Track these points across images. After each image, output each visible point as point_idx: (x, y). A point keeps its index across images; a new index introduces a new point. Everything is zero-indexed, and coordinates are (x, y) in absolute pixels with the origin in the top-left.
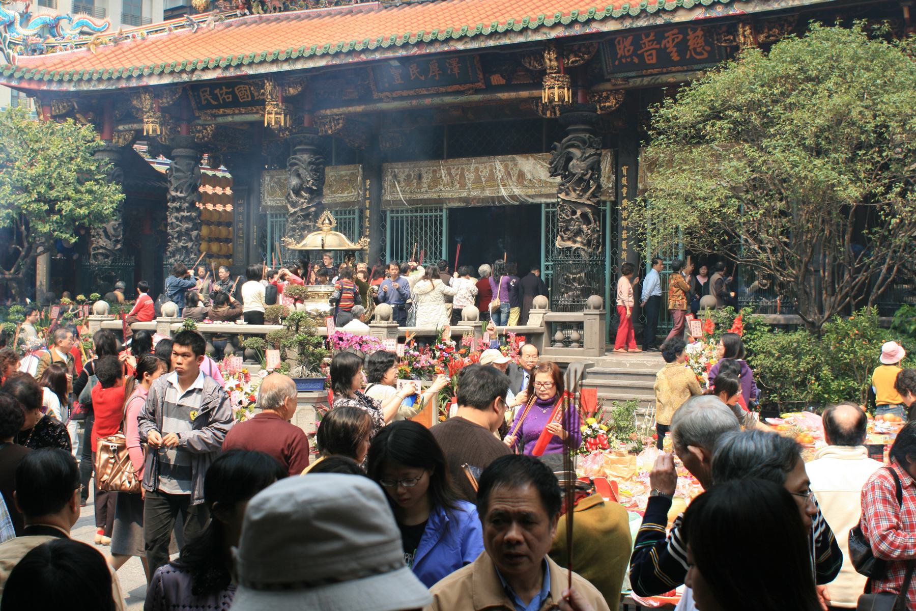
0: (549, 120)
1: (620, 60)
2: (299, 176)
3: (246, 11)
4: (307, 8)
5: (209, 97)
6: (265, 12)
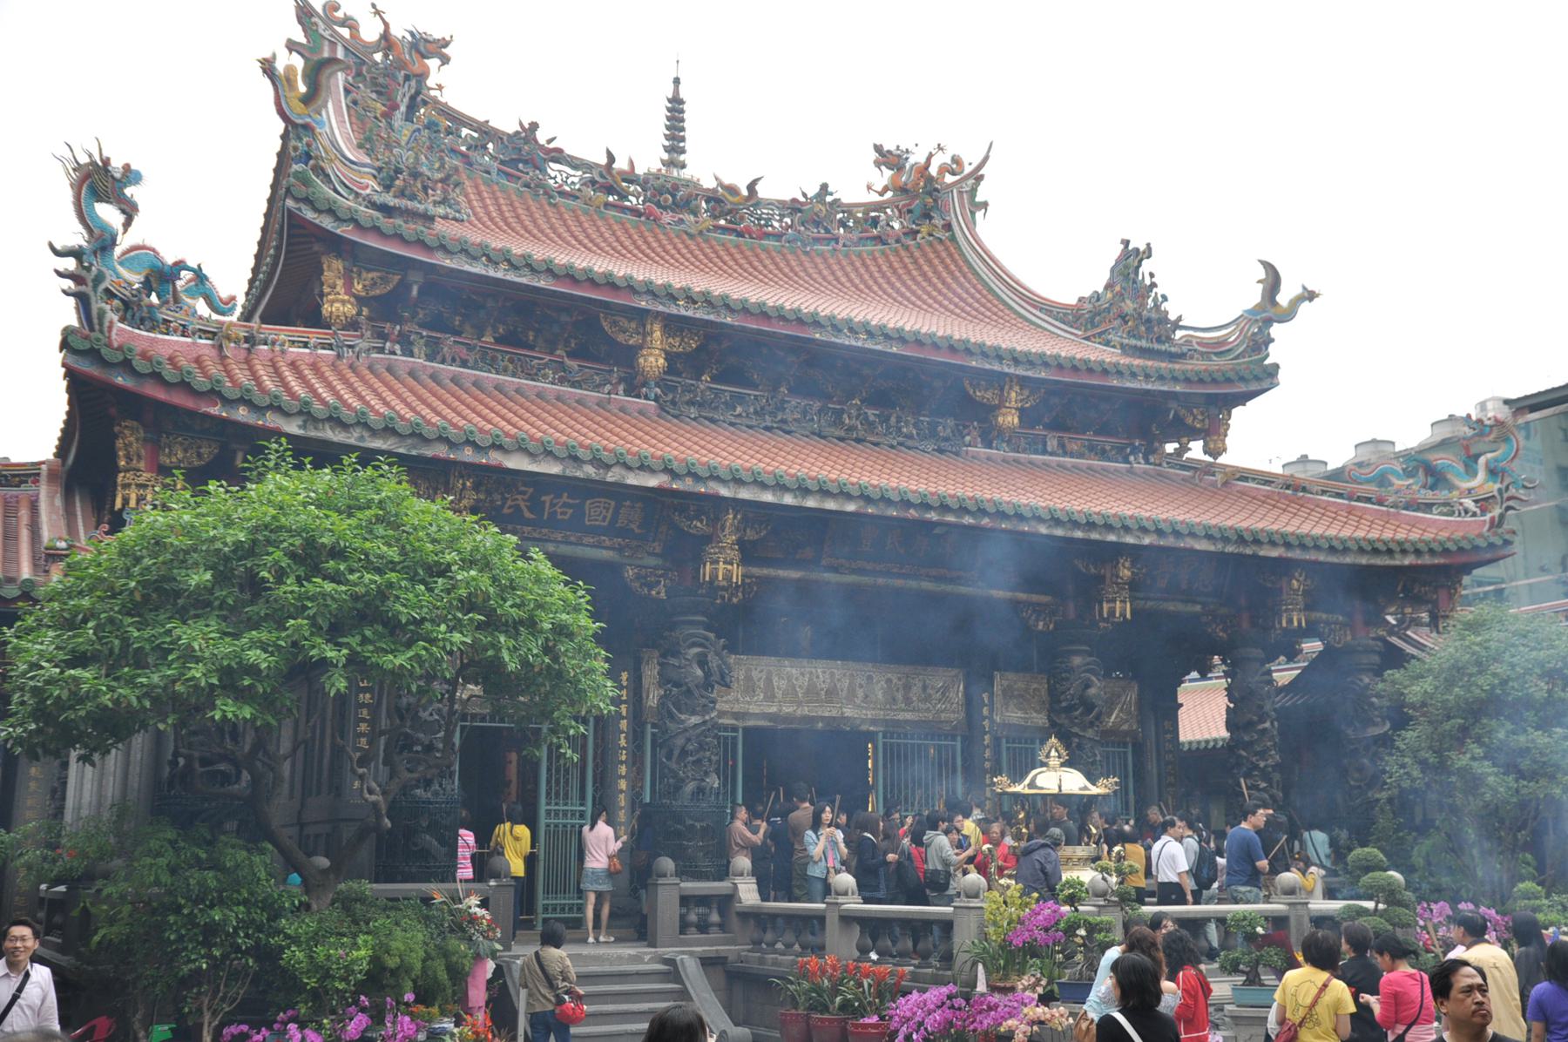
0: (1041, 632)
2: (702, 662)
3: (397, 347)
5: (522, 504)
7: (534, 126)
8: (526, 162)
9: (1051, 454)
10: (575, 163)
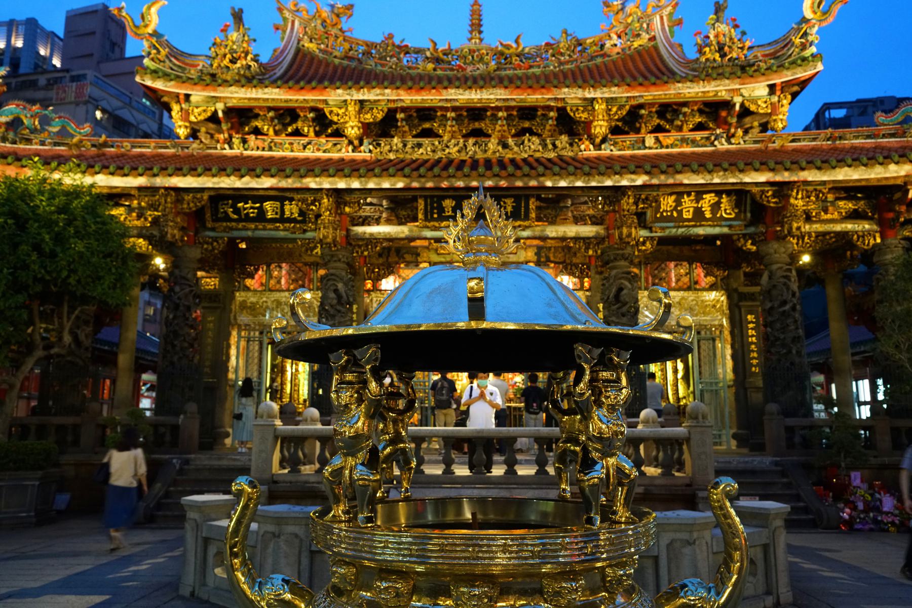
1: (662, 213)
3: (226, 146)
4: (292, 151)
6: (246, 150)
7: (391, 36)
8: (391, 57)
9: (650, 148)
10: (418, 51)
